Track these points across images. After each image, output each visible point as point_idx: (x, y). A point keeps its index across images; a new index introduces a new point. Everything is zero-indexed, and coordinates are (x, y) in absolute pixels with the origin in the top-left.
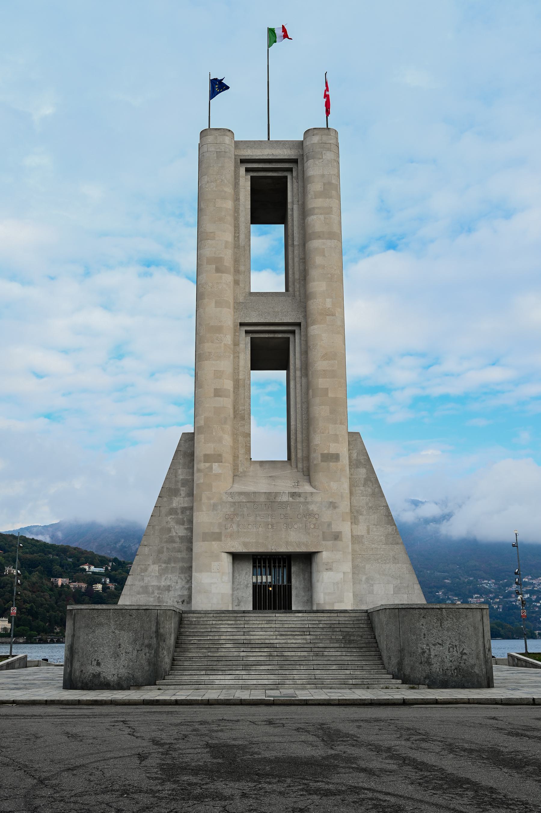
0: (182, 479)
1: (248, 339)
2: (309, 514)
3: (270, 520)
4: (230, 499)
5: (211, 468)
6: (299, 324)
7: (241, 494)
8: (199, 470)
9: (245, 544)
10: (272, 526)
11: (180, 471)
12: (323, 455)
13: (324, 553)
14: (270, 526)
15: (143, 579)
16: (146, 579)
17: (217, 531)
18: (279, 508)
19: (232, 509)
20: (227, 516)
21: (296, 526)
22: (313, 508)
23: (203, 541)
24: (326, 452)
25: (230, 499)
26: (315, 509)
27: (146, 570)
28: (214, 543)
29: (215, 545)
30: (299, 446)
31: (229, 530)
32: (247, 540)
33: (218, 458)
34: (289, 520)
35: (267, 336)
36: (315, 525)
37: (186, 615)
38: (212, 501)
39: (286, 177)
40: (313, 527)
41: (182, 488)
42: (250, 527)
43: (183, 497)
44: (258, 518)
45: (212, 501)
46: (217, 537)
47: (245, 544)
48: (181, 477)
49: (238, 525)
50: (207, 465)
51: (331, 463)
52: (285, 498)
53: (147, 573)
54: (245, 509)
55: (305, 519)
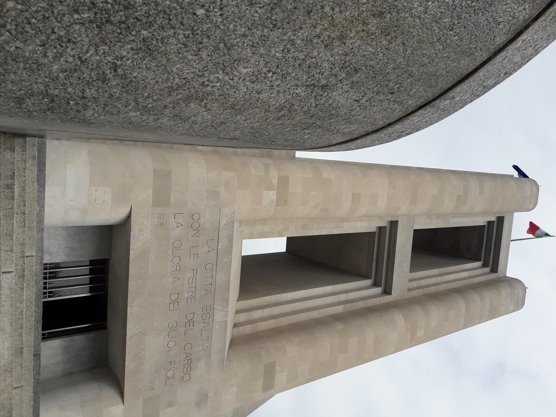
1: (374, 230)
2: (189, 363)
3: (186, 295)
4: (223, 222)
5: (270, 188)
6: (387, 291)
8: (267, 167)
10: (175, 302)
12: (273, 364)
13: (122, 405)
14: (174, 297)
17: (173, 199)
18: (204, 310)
20: (196, 217)
21: (171, 344)
23: (155, 171)
24: (277, 368)
28: (151, 191)
29: (143, 195)
30: (267, 312)
31: (172, 220)
33: (282, 200)
34: (183, 330)
35: (375, 251)
36: (173, 377)
37: (32, 151)
38: (222, 190)
39: (479, 260)
40: (169, 375)
42: (176, 260)
44: (189, 274)
45: (222, 190)
46: (161, 199)
50: (275, 181)
51: (262, 380)
52: (218, 316)
54: (206, 249)
55: (183, 357)
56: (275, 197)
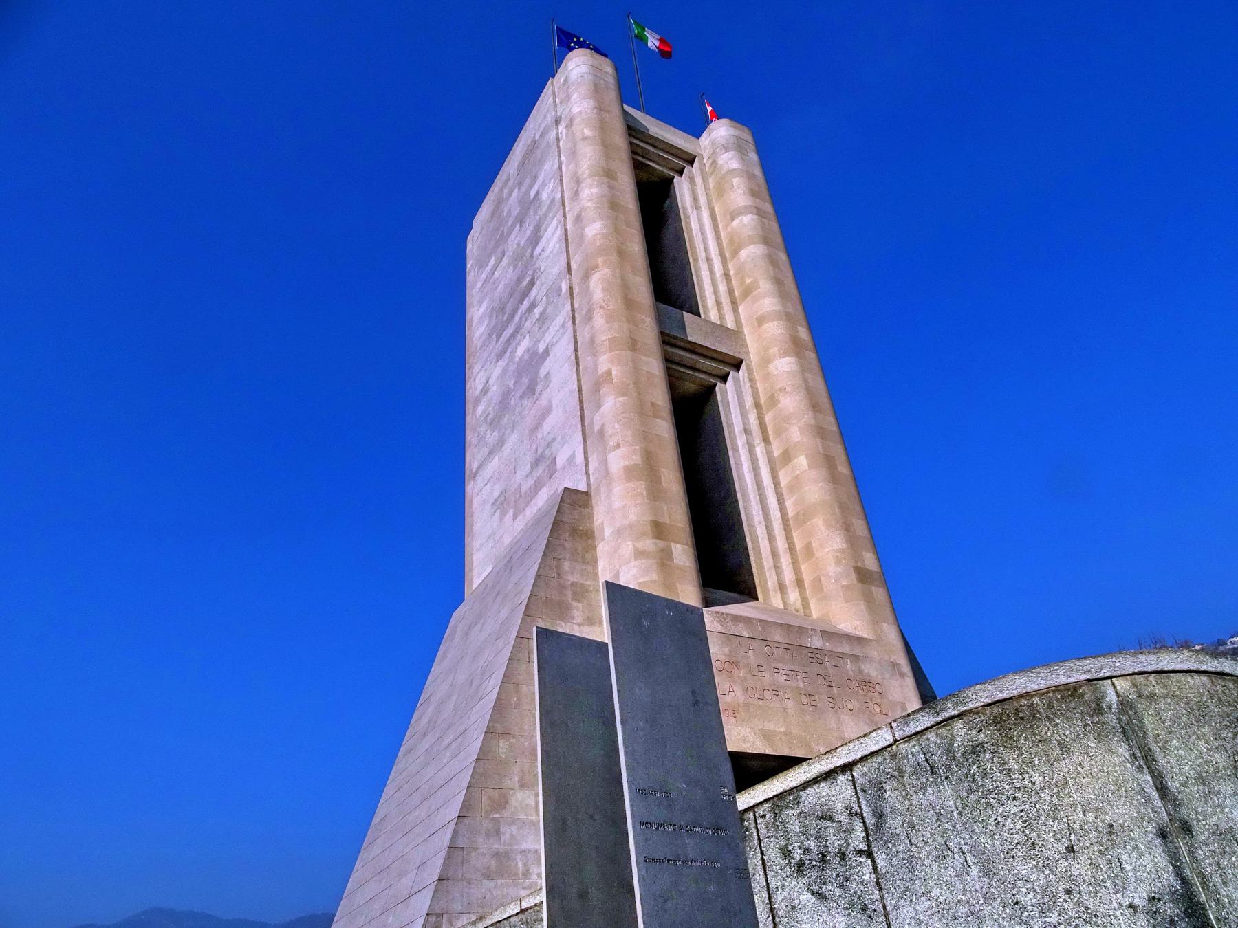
0: (573, 584)
2: (866, 683)
4: (719, 628)
7: (736, 619)
9: (767, 736)
11: (566, 566)
15: (498, 832)
16: (507, 832)
19: (726, 650)
22: (871, 670)
24: (860, 564)
25: (719, 628)
26: (874, 674)
27: (501, 803)
32: (771, 726)
41: (575, 604)
42: (768, 695)
43: (579, 625)
47: (767, 736)
48: (571, 578)
49: (746, 689)
50: (661, 544)
52: (817, 642)
53: (506, 814)
56: (678, 546)
